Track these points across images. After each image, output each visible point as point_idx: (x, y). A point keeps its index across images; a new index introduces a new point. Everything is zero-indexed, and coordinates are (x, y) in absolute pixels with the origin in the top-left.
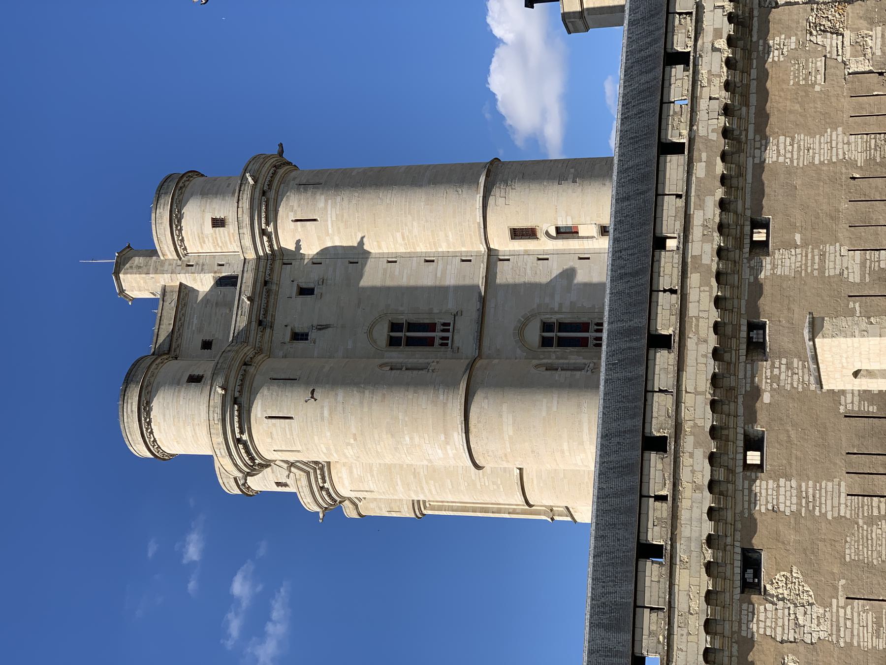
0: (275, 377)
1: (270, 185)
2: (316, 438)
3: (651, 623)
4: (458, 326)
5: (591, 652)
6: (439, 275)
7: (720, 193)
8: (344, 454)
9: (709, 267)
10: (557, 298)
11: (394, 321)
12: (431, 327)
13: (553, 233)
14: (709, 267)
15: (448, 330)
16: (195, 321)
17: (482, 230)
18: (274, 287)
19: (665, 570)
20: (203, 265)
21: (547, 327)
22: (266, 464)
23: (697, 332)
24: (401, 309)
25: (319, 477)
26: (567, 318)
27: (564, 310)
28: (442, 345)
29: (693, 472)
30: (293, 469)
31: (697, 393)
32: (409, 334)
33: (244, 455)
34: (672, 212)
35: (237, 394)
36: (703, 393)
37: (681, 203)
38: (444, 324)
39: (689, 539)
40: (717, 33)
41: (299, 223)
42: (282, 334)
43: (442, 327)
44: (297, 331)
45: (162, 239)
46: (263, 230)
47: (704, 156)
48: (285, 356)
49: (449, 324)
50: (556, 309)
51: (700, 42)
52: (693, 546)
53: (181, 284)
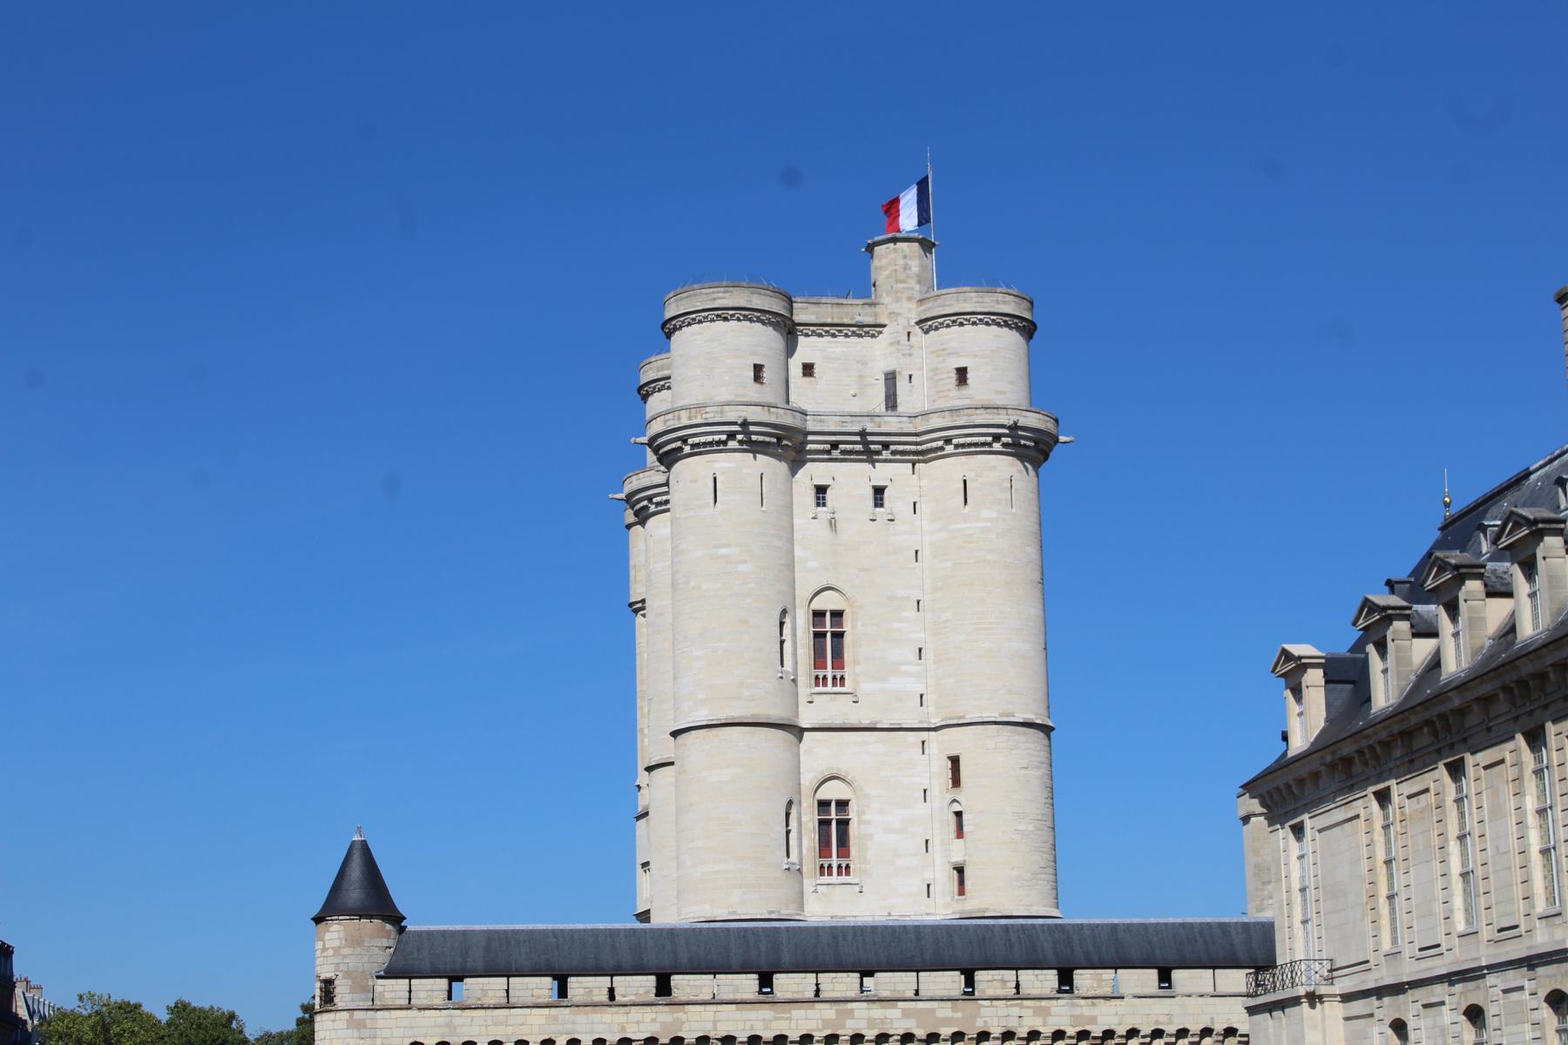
3: (494, 987)
5: (464, 933)
6: (904, 668)
7: (921, 1033)
9: (843, 1027)
13: (957, 807)
14: (843, 1027)
15: (834, 685)
16: (838, 350)
19: (547, 1000)
21: (843, 805)
23: (776, 1019)
26: (853, 829)
28: (817, 678)
29: (638, 1022)
31: (715, 1022)
34: (900, 987)
35: (740, 437)
36: (715, 1029)
37: (911, 994)
38: (842, 678)
39: (574, 1023)
40: (1093, 1020)
45: (939, 301)
47: (959, 1015)
49: (842, 685)
51: (1083, 1002)
52: (569, 1026)
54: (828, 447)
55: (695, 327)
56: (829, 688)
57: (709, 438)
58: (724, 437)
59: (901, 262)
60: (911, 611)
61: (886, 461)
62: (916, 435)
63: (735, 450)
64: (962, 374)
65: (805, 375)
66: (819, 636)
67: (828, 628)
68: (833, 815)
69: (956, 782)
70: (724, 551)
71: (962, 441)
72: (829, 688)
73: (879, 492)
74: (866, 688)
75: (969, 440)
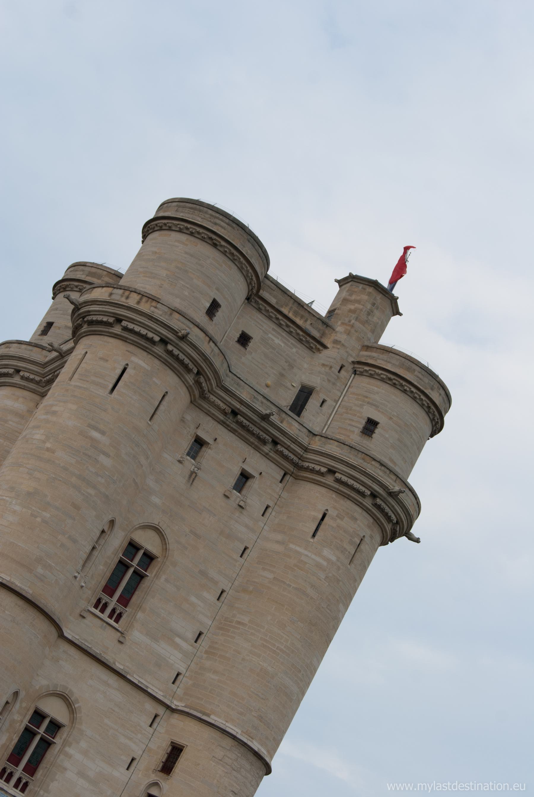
0: (166, 398)
1: (378, 507)
2: (74, 407)
4: (109, 630)
6: (178, 640)
8: (38, 427)
10: (78, 756)
11: (154, 562)
12: (124, 601)
15: (110, 616)
16: (277, 341)
17: (199, 715)
18: (267, 449)
20: (334, 384)
22: (77, 334)
24: (163, 577)
25: (32, 376)
27: (62, 757)
28: (99, 601)
30: (54, 354)
32: (131, 571)
33: (100, 318)
35: (170, 347)
38: (120, 616)
41: (320, 516)
42: (209, 429)
43: (118, 612)
44: (204, 449)
46: (334, 472)
48: (183, 420)
49: (117, 621)
50: (67, 749)
53: (325, 347)
54: (229, 410)
55: (183, 237)
56: (105, 616)
57: (144, 332)
58: (157, 339)
59: (369, 306)
60: (211, 597)
61: (266, 455)
62: (306, 450)
63: (158, 357)
64: (370, 426)
65: (239, 341)
66: (123, 565)
67: (135, 563)
68: (42, 730)
69: (167, 768)
70: (95, 434)
71: (344, 479)
72: (105, 616)
73: (245, 477)
74: (137, 635)
75: (351, 482)
